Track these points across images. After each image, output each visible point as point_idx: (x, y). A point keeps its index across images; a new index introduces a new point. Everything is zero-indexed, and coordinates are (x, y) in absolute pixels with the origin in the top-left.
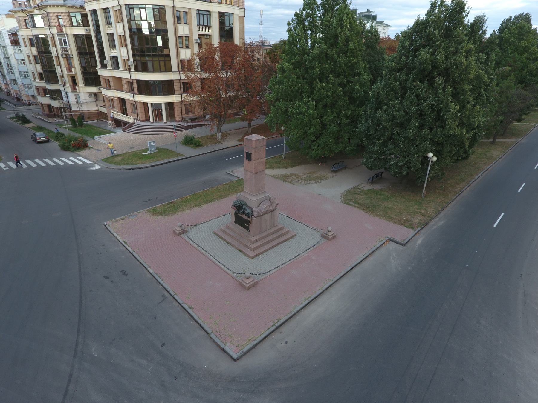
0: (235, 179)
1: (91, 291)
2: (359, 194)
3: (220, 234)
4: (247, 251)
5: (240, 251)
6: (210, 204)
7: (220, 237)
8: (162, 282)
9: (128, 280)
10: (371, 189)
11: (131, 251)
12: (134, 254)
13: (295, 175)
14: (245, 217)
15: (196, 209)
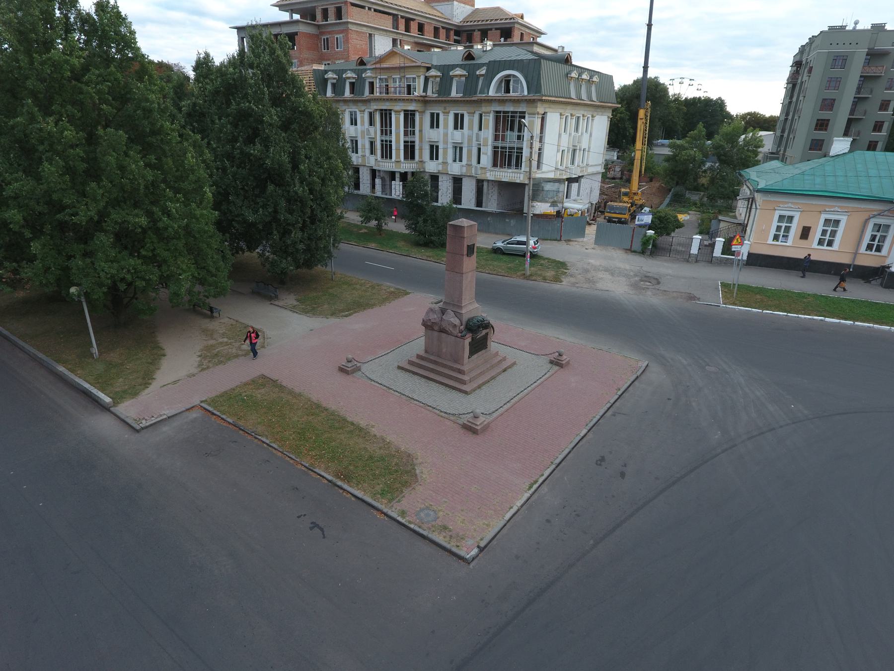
0: (194, 415)
1: (657, 478)
2: (314, 308)
3: (474, 385)
4: (504, 365)
5: (504, 370)
6: (349, 419)
7: (479, 387)
8: (598, 417)
9: (611, 452)
10: (298, 300)
11: (553, 466)
12: (558, 461)
13: (211, 346)
14: (484, 332)
15: (374, 431)
